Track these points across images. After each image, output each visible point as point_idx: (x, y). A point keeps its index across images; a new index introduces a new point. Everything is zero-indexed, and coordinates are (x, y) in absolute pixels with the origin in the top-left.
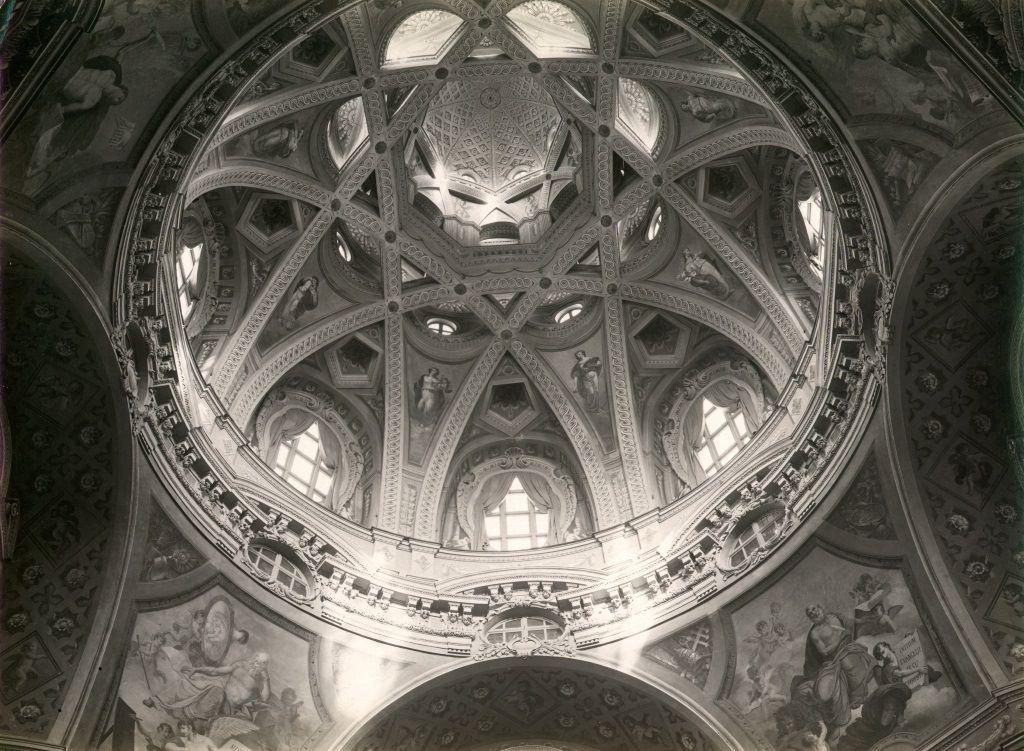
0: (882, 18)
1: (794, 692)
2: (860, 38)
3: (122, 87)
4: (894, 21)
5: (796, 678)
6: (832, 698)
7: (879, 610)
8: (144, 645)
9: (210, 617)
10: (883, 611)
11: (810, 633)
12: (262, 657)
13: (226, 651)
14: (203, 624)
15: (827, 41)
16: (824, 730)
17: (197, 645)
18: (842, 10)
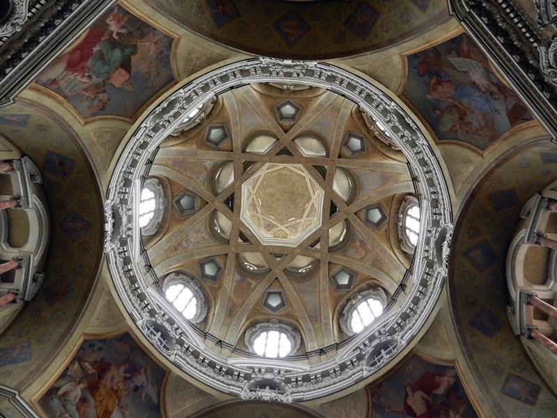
0: (116, 388)
1: (135, 48)
2: (125, 373)
3: (406, 391)
4: (112, 389)
5: (136, 54)
6: (113, 49)
7: (92, 96)
8: (487, 135)
9: (449, 126)
10: (90, 96)
11: (130, 73)
12: (429, 97)
13: (446, 108)
14: (454, 126)
15: (138, 368)
16: (114, 36)
17: (461, 118)
18: (132, 385)
